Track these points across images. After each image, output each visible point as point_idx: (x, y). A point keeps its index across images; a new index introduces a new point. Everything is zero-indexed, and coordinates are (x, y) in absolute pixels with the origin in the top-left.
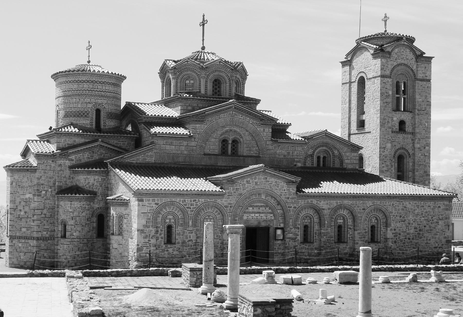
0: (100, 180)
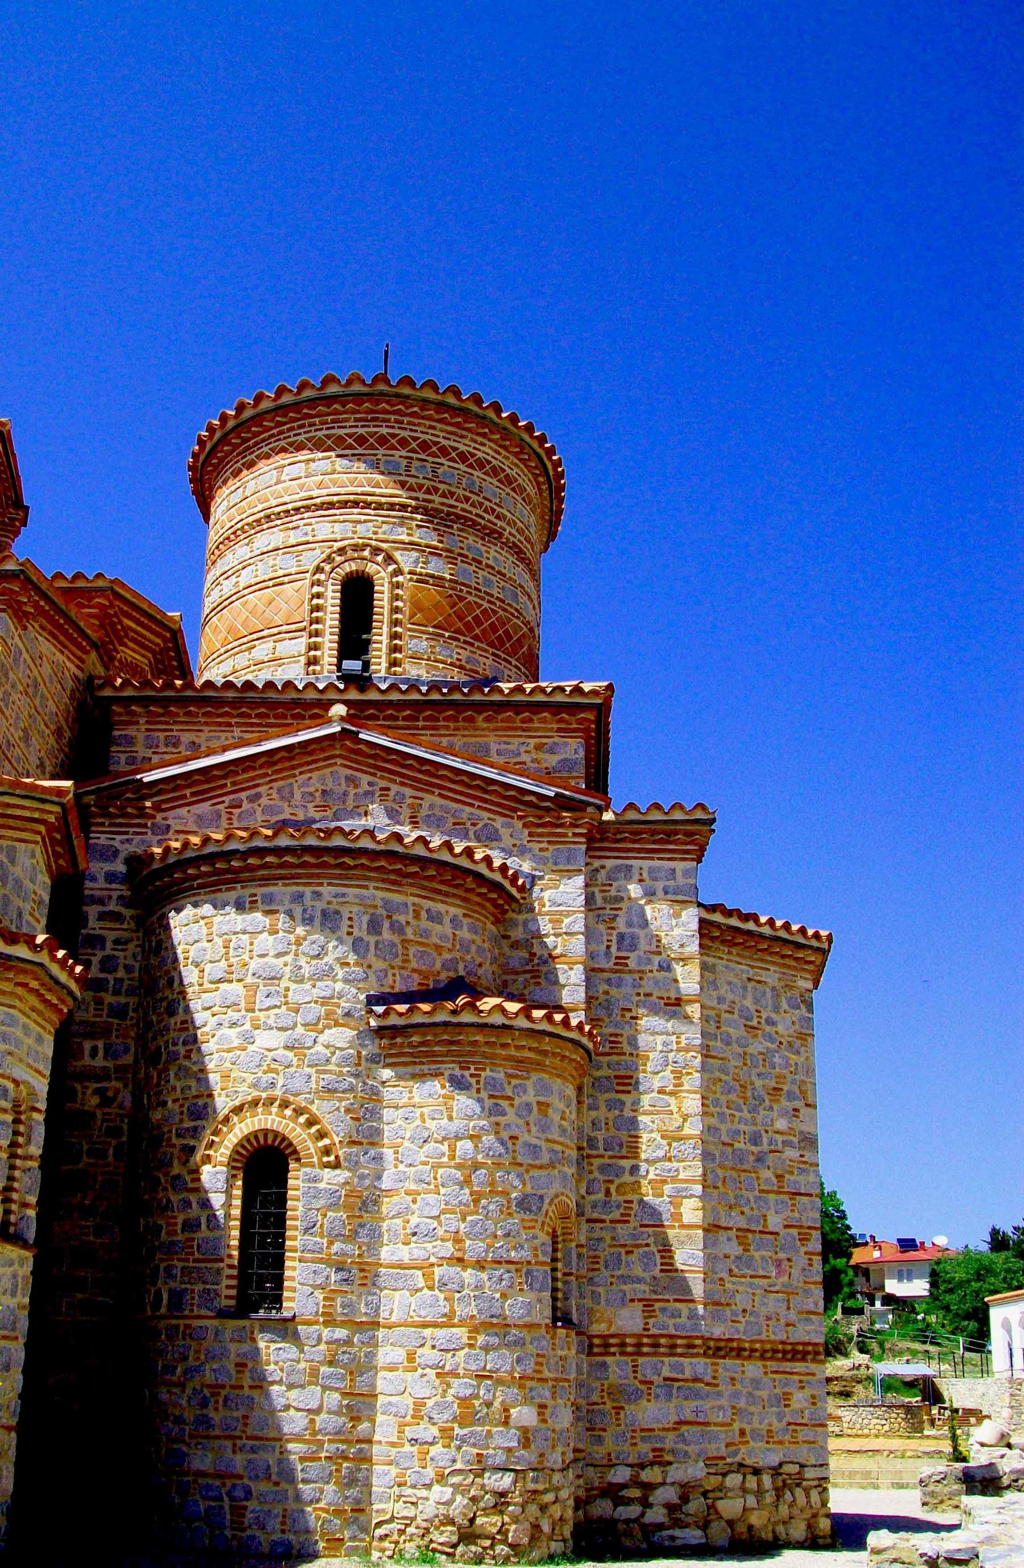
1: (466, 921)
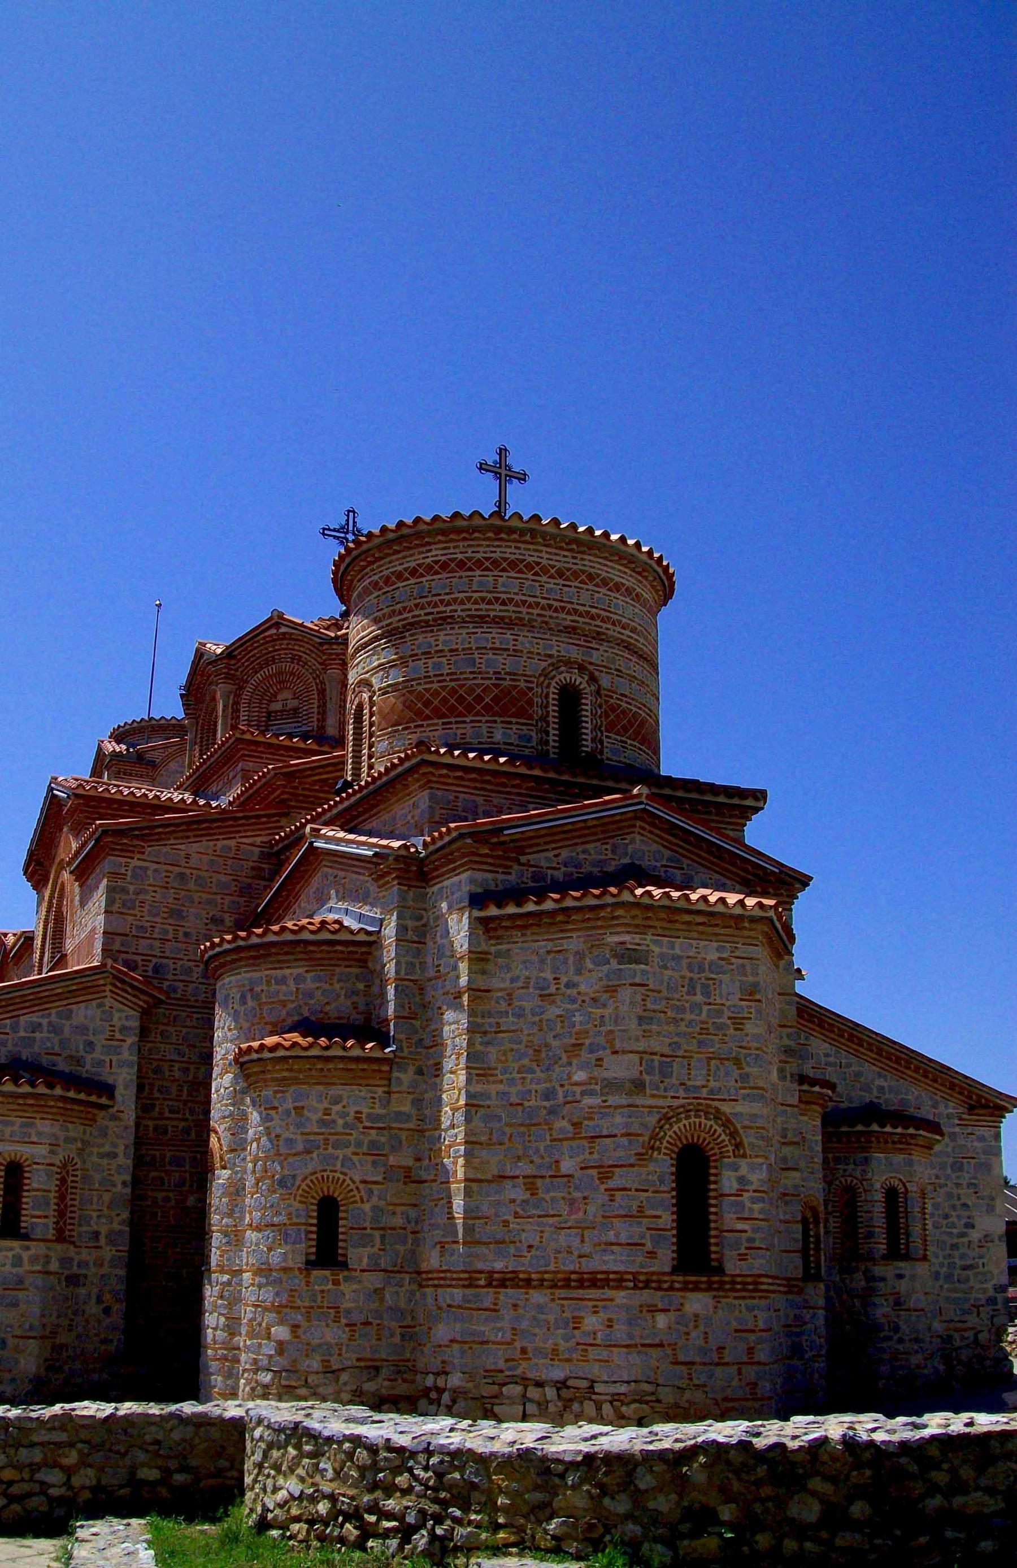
1: (309, 976)
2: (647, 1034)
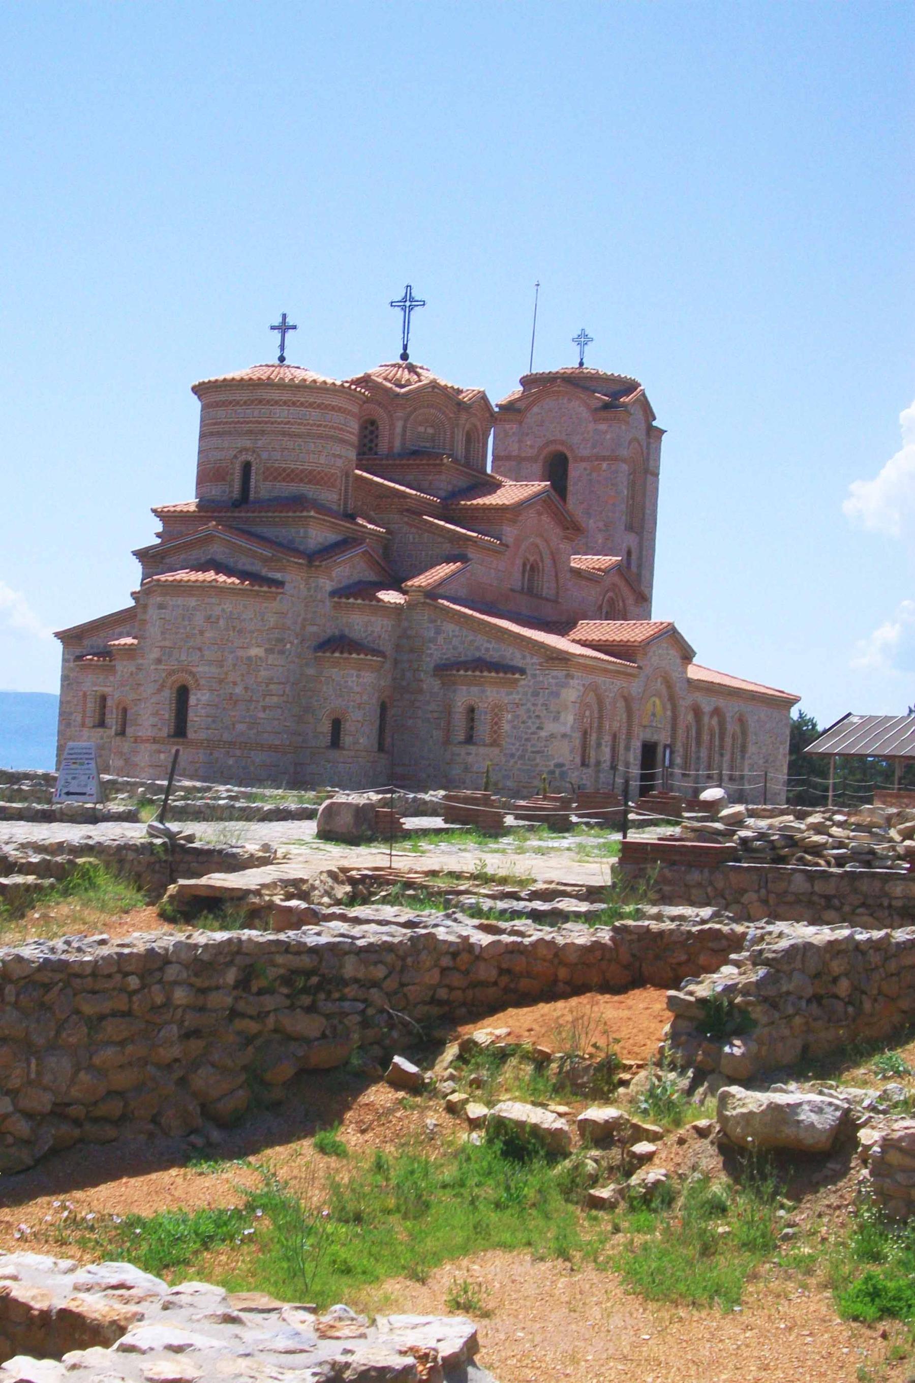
0: (390, 629)
2: (165, 639)
